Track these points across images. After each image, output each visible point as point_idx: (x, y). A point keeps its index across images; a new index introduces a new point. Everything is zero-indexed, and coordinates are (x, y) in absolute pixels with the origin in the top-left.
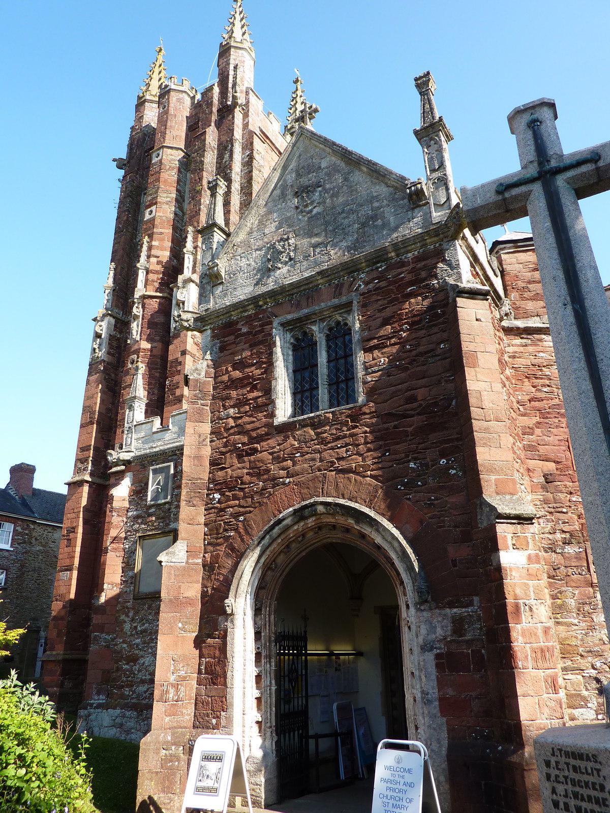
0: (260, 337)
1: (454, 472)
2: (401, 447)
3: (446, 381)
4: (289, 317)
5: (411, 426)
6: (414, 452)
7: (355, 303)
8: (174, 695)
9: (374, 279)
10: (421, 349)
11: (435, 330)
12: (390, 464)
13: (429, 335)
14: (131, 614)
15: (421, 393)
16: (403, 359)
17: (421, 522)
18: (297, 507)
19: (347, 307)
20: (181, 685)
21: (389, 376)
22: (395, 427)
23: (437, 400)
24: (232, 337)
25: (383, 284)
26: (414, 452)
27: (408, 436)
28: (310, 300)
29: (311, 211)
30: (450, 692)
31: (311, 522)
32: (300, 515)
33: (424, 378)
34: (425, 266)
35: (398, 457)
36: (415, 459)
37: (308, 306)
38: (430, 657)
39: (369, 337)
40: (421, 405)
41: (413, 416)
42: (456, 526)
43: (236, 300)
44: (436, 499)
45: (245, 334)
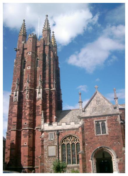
0: (92, 122)
2: (113, 140)
7: (106, 121)
10: (116, 129)
14: (47, 159)
15: (116, 134)
18: (100, 147)
19: (105, 121)
24: (87, 121)
30: (119, 167)
31: (101, 149)
32: (100, 148)
38: (117, 163)
43: (87, 116)
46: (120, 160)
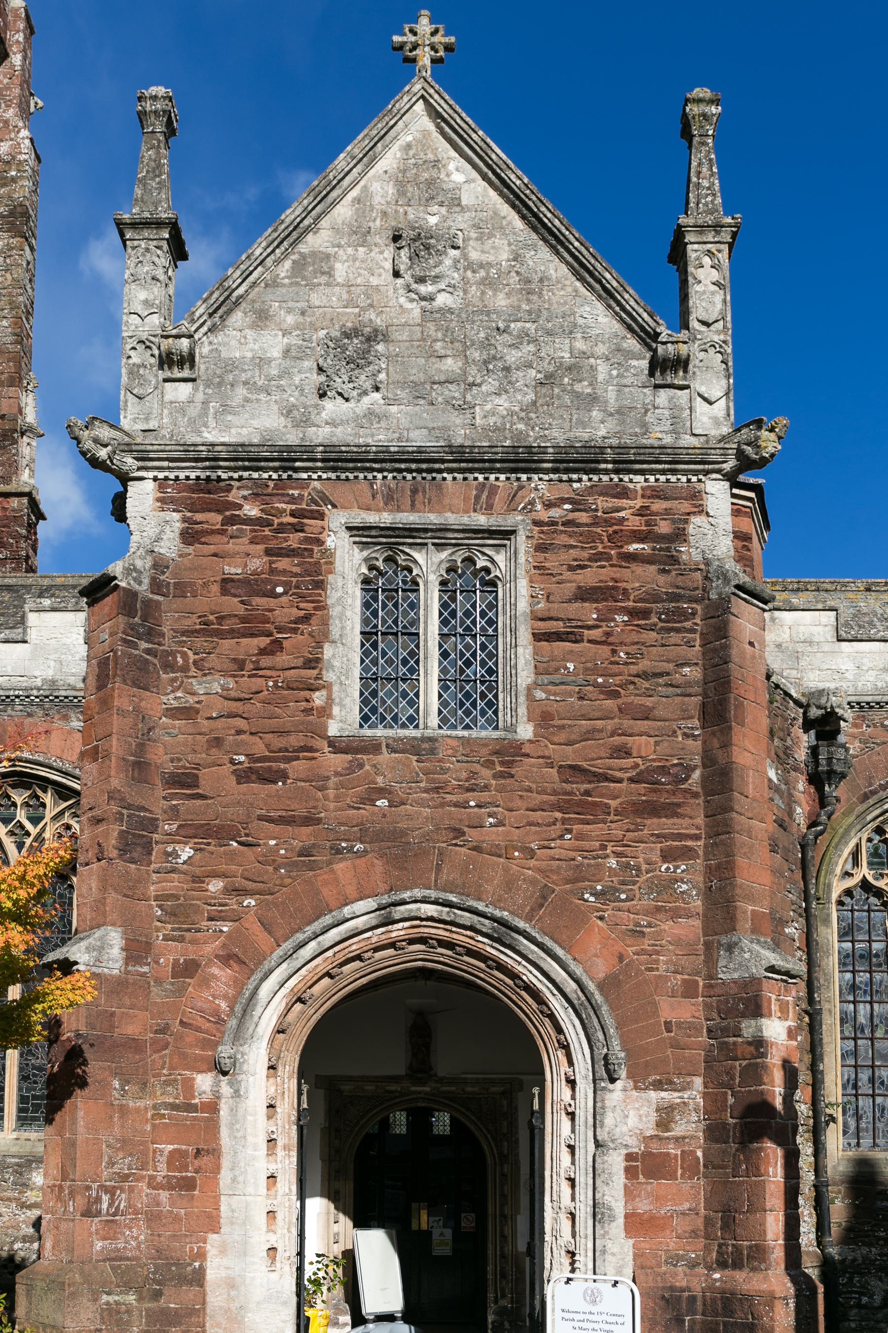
1: (685, 887)
3: (686, 736)
4: (372, 518)
5: (615, 798)
6: (619, 842)
7: (521, 537)
8: (110, 1205)
9: (564, 500)
10: (644, 665)
11: (674, 638)
12: (572, 854)
13: (663, 645)
16: (611, 676)
17: (621, 958)
20: (122, 1190)
21: (581, 698)
22: (587, 793)
23: (668, 764)
25: (583, 517)
26: (619, 842)
27: (609, 814)
28: (419, 496)
29: (430, 298)
33: (647, 718)
34: (667, 512)
35: (586, 844)
36: (617, 855)
37: (413, 508)
39: (547, 615)
40: (637, 765)
41: (620, 781)
42: (676, 972)
44: (649, 925)
45: (248, 521)
46: (665, 1117)
